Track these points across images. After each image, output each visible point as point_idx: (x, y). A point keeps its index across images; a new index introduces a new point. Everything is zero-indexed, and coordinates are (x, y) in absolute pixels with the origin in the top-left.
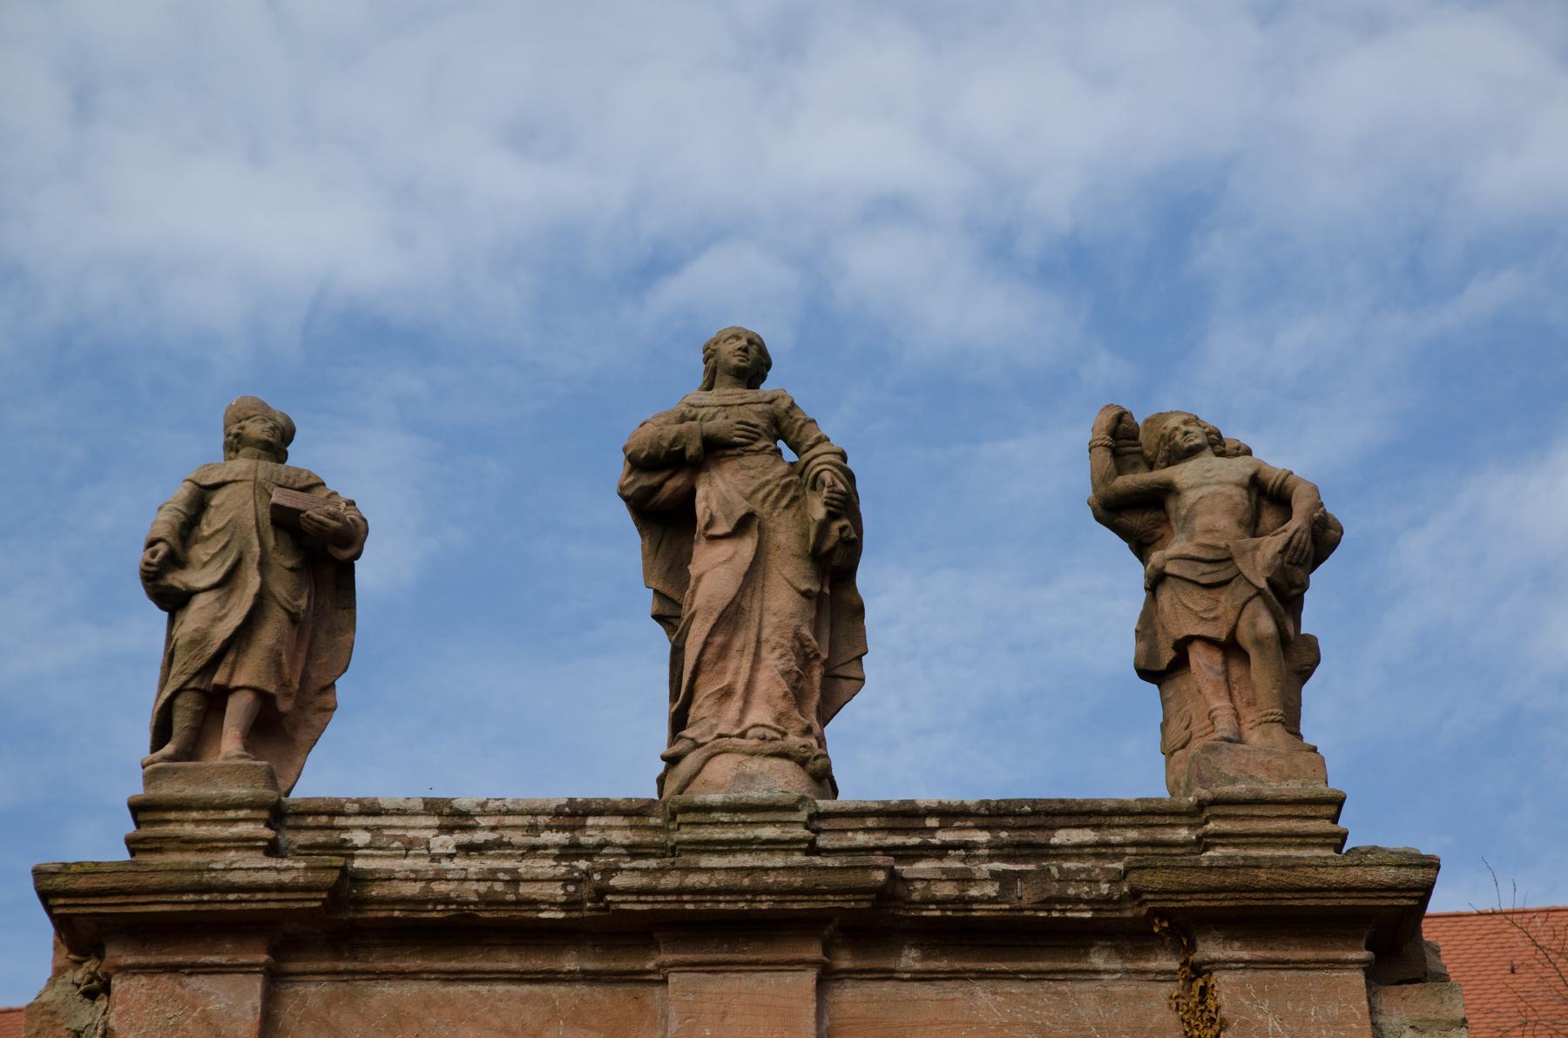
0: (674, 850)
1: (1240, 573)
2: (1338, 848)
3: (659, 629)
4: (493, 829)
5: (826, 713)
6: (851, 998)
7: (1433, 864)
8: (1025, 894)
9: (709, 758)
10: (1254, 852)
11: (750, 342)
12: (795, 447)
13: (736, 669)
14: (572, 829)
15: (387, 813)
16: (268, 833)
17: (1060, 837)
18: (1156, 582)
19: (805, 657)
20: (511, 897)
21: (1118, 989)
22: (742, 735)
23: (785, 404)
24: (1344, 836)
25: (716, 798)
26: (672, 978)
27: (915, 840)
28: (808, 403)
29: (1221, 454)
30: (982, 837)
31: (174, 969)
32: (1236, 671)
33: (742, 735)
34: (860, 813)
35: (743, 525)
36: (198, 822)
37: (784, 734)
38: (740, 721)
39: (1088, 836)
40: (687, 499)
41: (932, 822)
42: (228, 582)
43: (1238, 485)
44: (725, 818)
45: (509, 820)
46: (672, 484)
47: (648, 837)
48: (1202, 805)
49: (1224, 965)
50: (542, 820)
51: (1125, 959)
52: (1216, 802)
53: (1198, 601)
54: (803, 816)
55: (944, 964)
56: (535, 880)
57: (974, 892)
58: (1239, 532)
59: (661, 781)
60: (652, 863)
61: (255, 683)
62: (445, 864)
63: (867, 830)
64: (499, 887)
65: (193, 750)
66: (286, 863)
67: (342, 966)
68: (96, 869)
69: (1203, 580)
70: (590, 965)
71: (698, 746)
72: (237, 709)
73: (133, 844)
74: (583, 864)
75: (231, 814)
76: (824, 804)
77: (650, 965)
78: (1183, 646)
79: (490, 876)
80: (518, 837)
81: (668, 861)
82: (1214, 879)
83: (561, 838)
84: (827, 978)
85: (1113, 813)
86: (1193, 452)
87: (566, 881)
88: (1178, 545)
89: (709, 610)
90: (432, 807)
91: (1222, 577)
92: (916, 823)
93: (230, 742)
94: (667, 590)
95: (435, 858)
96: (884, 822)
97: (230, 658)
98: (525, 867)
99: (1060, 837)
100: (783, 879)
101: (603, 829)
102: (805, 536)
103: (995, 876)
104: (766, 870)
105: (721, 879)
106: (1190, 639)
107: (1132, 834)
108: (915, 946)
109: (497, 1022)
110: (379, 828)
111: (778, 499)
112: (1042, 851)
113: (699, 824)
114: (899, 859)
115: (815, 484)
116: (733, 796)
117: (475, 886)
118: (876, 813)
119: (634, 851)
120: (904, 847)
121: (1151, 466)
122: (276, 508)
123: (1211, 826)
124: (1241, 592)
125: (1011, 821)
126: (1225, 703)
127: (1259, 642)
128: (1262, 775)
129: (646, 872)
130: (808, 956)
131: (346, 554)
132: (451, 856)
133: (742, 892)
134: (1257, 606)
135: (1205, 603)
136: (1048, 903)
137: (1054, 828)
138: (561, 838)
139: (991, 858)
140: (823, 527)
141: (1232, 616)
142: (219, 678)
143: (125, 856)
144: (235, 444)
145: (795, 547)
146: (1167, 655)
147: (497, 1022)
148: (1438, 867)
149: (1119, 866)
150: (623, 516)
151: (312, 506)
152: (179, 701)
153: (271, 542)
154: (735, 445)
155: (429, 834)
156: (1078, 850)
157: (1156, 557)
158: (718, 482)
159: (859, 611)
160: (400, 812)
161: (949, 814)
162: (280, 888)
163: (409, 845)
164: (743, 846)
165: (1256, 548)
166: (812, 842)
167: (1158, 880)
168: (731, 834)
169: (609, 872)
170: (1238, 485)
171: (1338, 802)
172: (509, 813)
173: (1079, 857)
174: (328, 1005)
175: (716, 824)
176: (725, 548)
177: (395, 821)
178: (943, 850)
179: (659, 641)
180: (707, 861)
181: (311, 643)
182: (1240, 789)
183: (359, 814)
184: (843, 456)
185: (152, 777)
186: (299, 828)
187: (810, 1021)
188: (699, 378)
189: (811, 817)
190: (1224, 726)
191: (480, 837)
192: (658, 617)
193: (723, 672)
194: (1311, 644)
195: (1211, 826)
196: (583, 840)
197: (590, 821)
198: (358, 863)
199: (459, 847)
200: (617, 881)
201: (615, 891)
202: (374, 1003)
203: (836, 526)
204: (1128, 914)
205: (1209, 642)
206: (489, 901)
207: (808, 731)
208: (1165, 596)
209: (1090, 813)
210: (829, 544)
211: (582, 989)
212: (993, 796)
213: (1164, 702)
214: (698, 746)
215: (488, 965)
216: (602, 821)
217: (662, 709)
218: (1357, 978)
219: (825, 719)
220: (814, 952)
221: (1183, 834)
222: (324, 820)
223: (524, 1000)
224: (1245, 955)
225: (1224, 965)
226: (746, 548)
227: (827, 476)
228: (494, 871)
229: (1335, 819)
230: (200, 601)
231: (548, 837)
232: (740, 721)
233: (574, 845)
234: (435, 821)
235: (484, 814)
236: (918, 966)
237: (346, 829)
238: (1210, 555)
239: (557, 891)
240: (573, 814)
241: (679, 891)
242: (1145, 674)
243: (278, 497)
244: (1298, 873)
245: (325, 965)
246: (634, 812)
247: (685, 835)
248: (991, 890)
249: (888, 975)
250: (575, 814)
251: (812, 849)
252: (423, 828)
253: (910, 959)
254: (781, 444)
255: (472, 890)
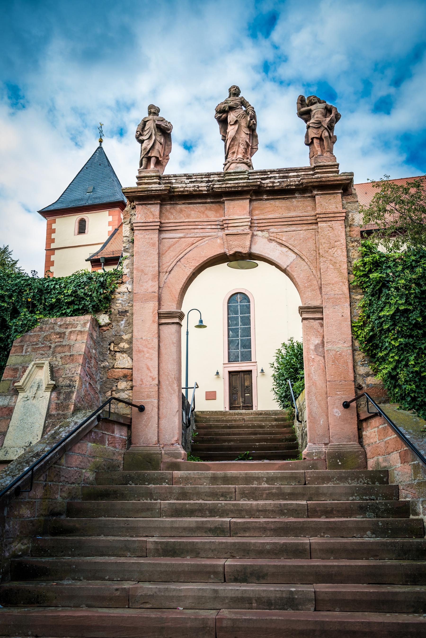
0: (225, 181)
1: (322, 125)
2: (338, 173)
3: (223, 142)
4: (195, 178)
5: (252, 154)
6: (255, 204)
7: (352, 174)
8: (284, 185)
9: (231, 164)
10: (323, 175)
11: (237, 88)
12: (245, 107)
13: (235, 149)
14: (208, 178)
15: (178, 177)
16: (159, 181)
17: (291, 174)
18: (308, 127)
19: (248, 145)
20: (198, 190)
21: (300, 200)
22: (236, 160)
23: (243, 99)
24: (339, 171)
25: (232, 171)
26: (225, 202)
27: (266, 176)
28: (247, 99)
29: (320, 103)
30: (277, 175)
31: (145, 204)
32: (322, 143)
33: (236, 160)
34: (256, 172)
35: (236, 122)
36: (147, 180)
37: (243, 159)
38: (236, 157)
39: (295, 174)
40: (226, 118)
41: (269, 173)
42: (150, 138)
43: (323, 109)
44: (234, 174)
45: (198, 177)
46: (224, 116)
47: (221, 178)
48: (315, 167)
49: (317, 194)
50: (203, 176)
51: (301, 195)
52: (317, 167)
53: (315, 131)
54: (247, 173)
55: (270, 197)
56: (202, 187)
57: (275, 185)
58: (323, 117)
59: (224, 168)
60: (221, 183)
61: (155, 155)
62: (188, 185)
63: (258, 175)
64: (196, 188)
65: (146, 168)
66: (161, 186)
67: (172, 202)
68: (131, 188)
69: (316, 127)
70: (212, 201)
71: (229, 162)
72: (153, 160)
73: (138, 184)
74: (210, 184)
75: (153, 178)
76: (250, 171)
77: (222, 200)
78: (312, 139)
79: (194, 187)
80: (199, 180)
81: (223, 182)
82: (315, 180)
83: (207, 179)
84: (251, 201)
85: (299, 170)
86: (315, 103)
87: (207, 187)
88: (312, 121)
89: (230, 138)
90: (185, 175)
91: (319, 126)
92: (266, 173)
93: (152, 166)
94: (224, 135)
95: (186, 184)
96: (260, 174)
97: (151, 151)
98: (200, 185)
99: (291, 174)
100: (243, 184)
101: (214, 177)
102: (247, 123)
103: (278, 182)
104: (240, 183)
105: (233, 185)
106: (314, 138)
107: (303, 173)
108: (265, 194)
109: (197, 210)
110: (177, 179)
111: (242, 117)
112: (287, 177)
113: (229, 176)
114: (262, 180)
115: (248, 114)
116: (235, 171)
117: (192, 188)
118: (259, 172)
119: (219, 181)
120: (264, 178)
121: (308, 106)
122: (156, 124)
123: (316, 171)
124: (322, 128)
125: (282, 172)
126: (320, 149)
127: (325, 137)
128: (325, 161)
129: (220, 184)
130: (247, 197)
131: (169, 132)
132: (189, 183)
133: (236, 187)
134: (325, 131)
135: (316, 131)
136: (287, 186)
137: (289, 173)
138: (207, 179)
139: (279, 179)
140: (250, 122)
141: (321, 133)
142: (149, 155)
143: (136, 185)
144: (150, 113)
145: (245, 126)
146: (310, 141)
147: (197, 210)
148: (353, 175)
149: (300, 179)
150: (216, 121)
151: (163, 124)
152: (143, 159)
153: (156, 131)
154: (234, 108)
155: (185, 180)
156: (294, 176)
157: (308, 123)
158: (231, 114)
159: (257, 136)
160: (180, 176)
161: (272, 172)
162: (160, 190)
163: (182, 182)
164: (237, 179)
165: (325, 120)
166: (248, 178)
167: (305, 181)
168: (235, 177)
169: (213, 185)
170: (323, 109)
171: (338, 165)
172: (198, 175)
173: (294, 177)
174: (170, 209)
175: (232, 175)
176: (233, 127)
177: (179, 178)
178: (270, 178)
179: (223, 143)
180: (229, 182)
181: (165, 148)
182: (321, 164)
183: (174, 177)
184: (253, 108)
185: (140, 172)
186: (164, 180)
187: (248, 208)
188: (228, 96)
189: (248, 173)
190: (319, 153)
191: (193, 180)
192: (222, 140)
193: (233, 149)
194: (335, 137)
195: (316, 171)
196: (210, 179)
197: (211, 176)
198: (174, 185)
199: (190, 182)
200: (215, 186)
201: (215, 188)
202: (178, 208)
203: (252, 121)
204: (301, 187)
205: (317, 138)
206: (195, 191)
207: (248, 158)
208: (310, 130)
209: (296, 170)
210: (251, 125)
211: (211, 205)
212: (279, 168)
213: (310, 149)
214: (229, 162)
215: (195, 201)
216: (213, 176)
217: (224, 156)
218: (340, 195)
219: (251, 156)
220: (249, 197)
221: (311, 172)
222: (168, 178)
223: (201, 207)
224: (321, 193)
225: (317, 194)
226: (236, 127)
227: (250, 112)
228: (195, 186)
229: (338, 168)
230: (145, 142)
231: (204, 179)
232: (236, 157)
233: (209, 180)
234: (186, 178)
235: (194, 176)
236: (266, 198)
237: (171, 180)
238: (317, 122)
239: (205, 188)
240: (208, 175)
241: (225, 187)
242: (307, 144)
243: (157, 122)
244: (330, 178)
245: (169, 202)
246: (219, 174)
247: (227, 178)
248: (278, 184)
249: (261, 200)
250: (208, 175)
251: (248, 179)
252: (184, 179)
253: (265, 197)
254: (243, 107)
255: (191, 189)
